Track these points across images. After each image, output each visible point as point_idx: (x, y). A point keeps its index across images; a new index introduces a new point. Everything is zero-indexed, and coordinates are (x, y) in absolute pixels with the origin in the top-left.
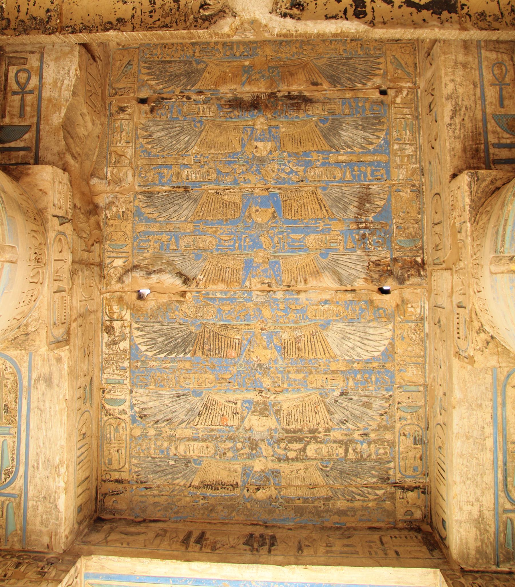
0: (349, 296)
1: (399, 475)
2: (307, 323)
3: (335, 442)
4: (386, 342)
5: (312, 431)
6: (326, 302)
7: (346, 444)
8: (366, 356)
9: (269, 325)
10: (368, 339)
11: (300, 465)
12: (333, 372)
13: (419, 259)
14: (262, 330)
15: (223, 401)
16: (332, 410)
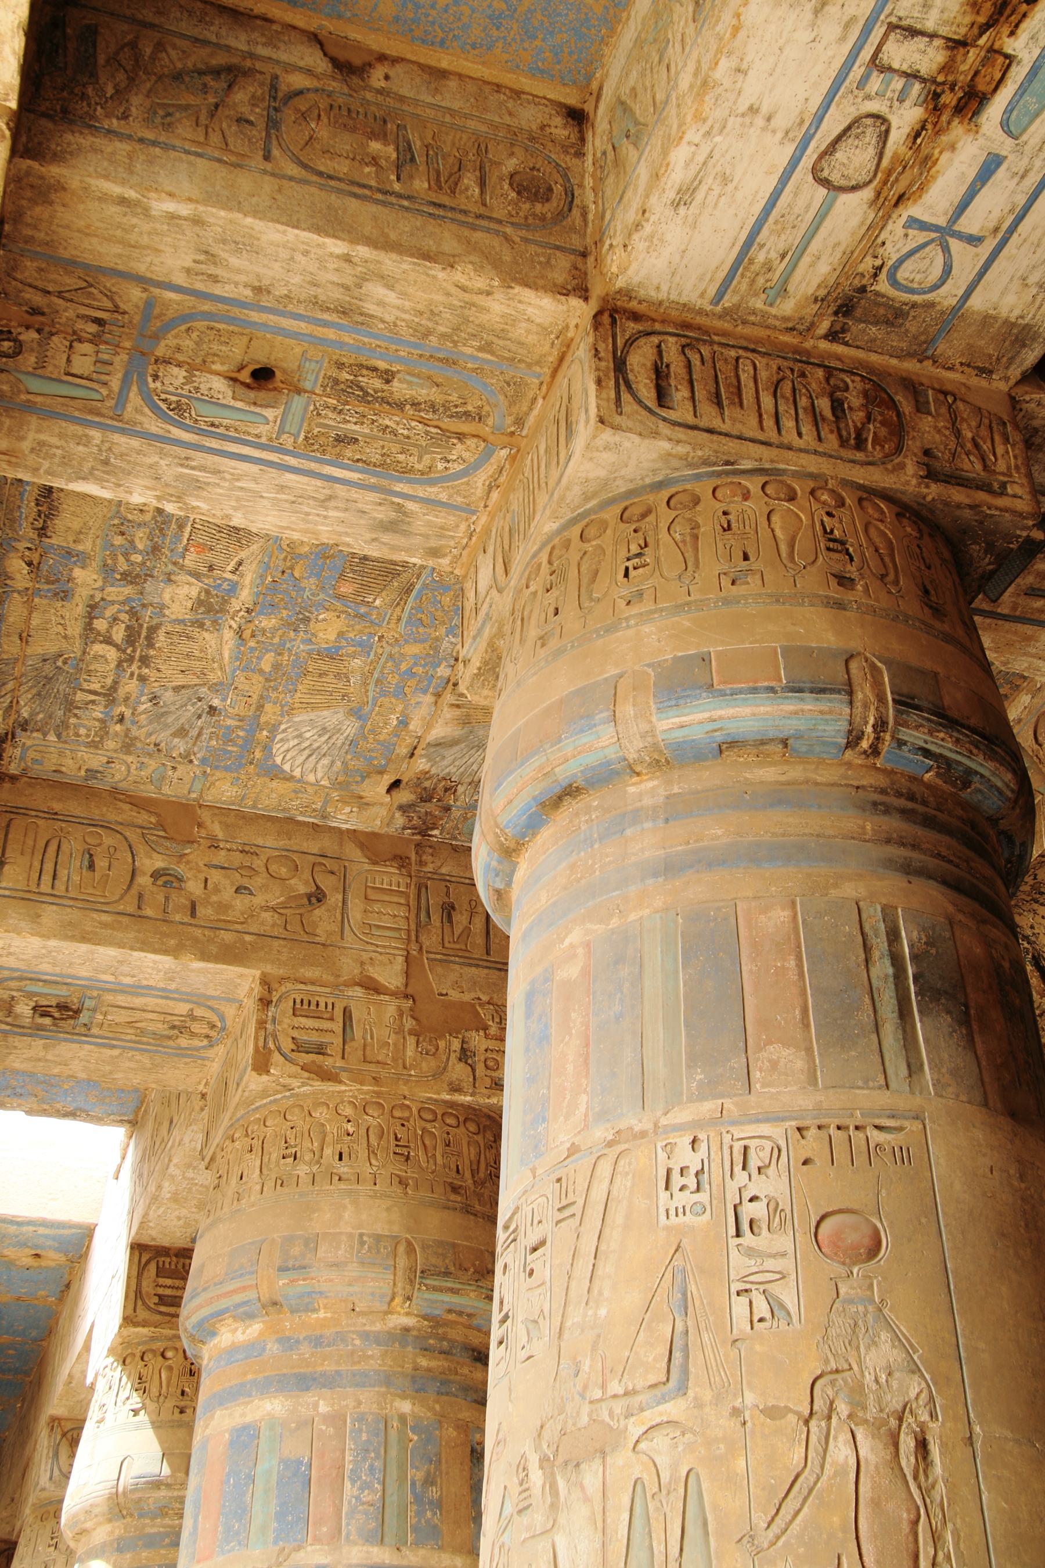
0: (404, 751)
1: (29, 743)
2: (371, 694)
3: (116, 683)
4: (297, 773)
5: (145, 661)
6: (404, 723)
7: (105, 695)
8: (278, 749)
9: (388, 649)
10: (310, 755)
11: (75, 629)
12: (260, 707)
13: (435, 832)
14: (381, 638)
15: (243, 554)
16: (183, 691)
